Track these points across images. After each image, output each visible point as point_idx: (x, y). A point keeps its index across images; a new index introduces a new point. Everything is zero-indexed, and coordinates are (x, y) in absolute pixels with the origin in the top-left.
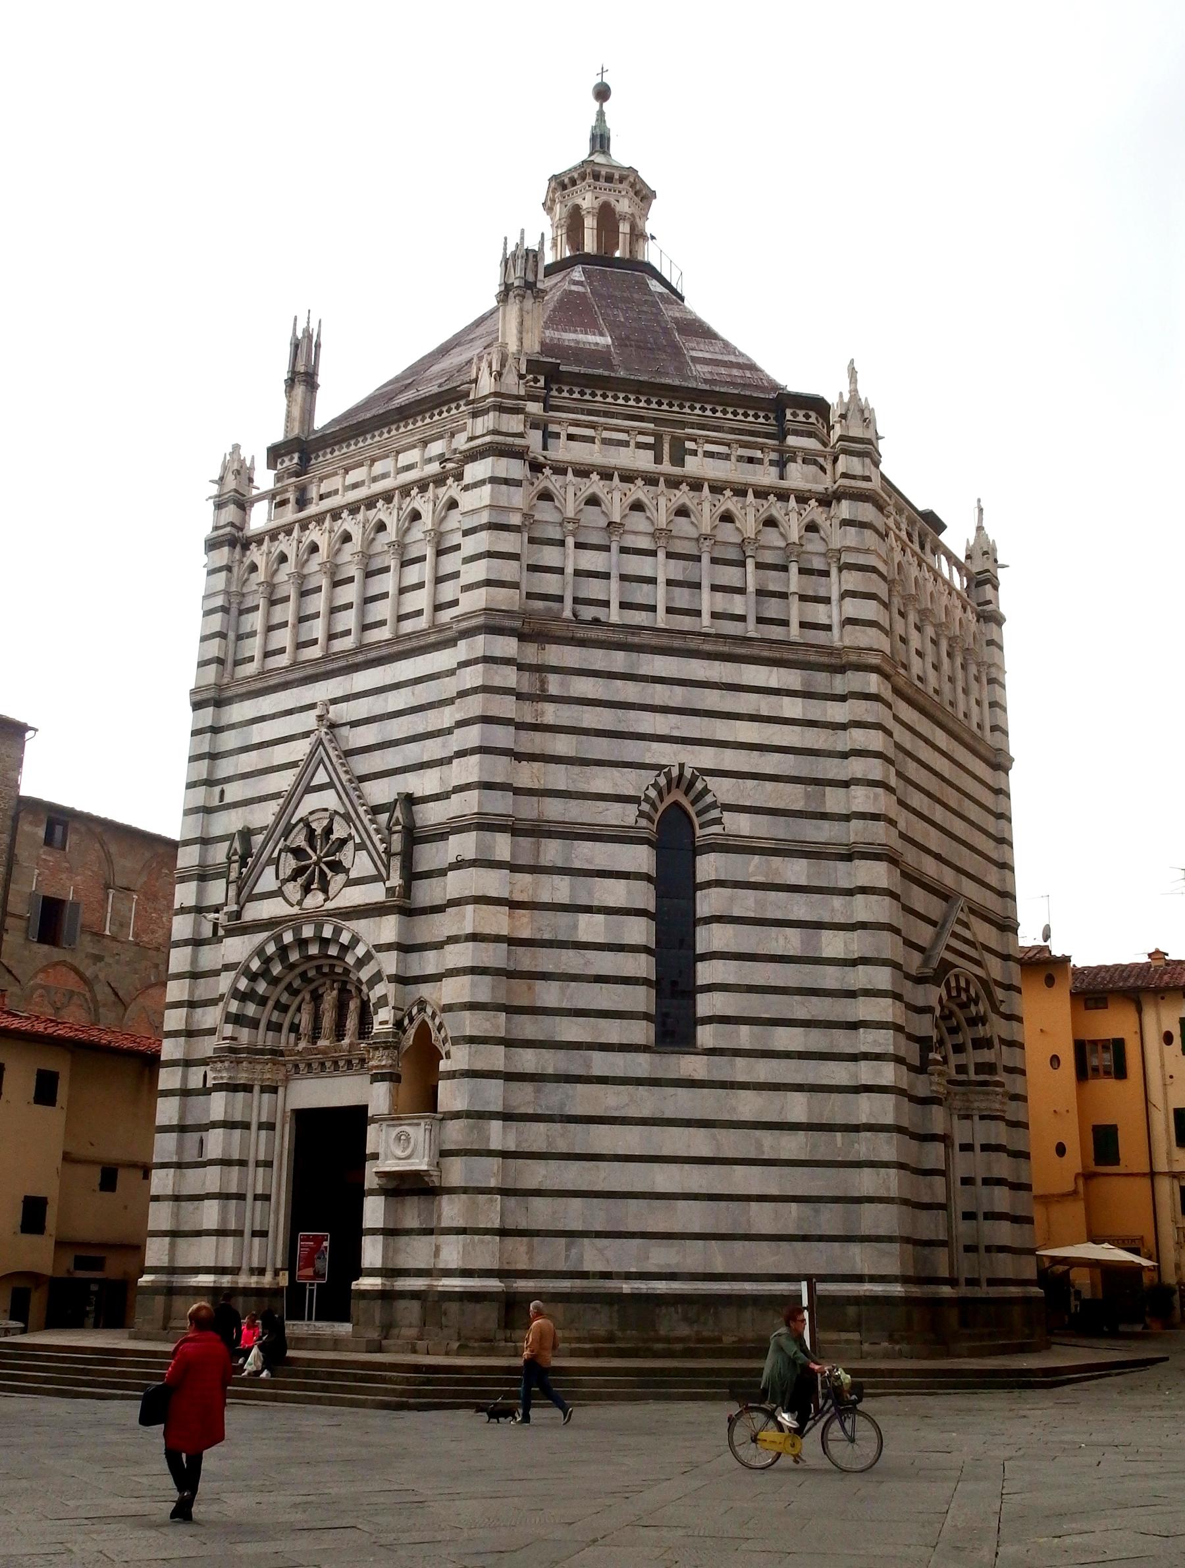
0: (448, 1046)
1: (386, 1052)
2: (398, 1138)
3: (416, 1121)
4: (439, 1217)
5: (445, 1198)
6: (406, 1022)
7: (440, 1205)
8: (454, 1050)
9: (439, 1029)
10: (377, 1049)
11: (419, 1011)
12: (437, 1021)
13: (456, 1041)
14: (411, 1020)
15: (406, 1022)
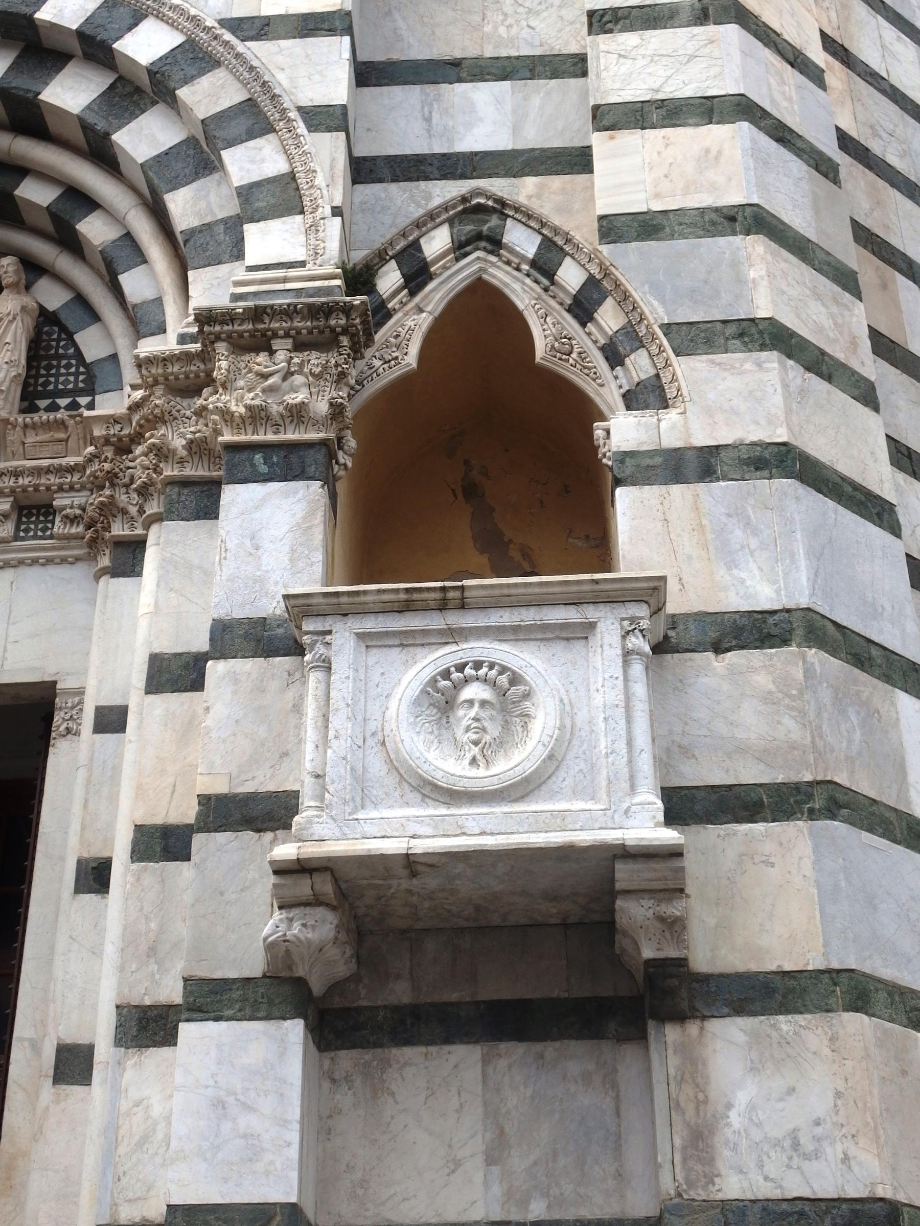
0: (640, 365)
1: (315, 360)
2: (441, 699)
3: (571, 615)
4: (700, 1141)
5: (727, 1042)
6: (389, 279)
7: (694, 1070)
8: (689, 371)
9: (583, 307)
10: (262, 344)
11: (460, 248)
12: (571, 276)
13: (693, 338)
14: (417, 275)
15: (389, 279)
